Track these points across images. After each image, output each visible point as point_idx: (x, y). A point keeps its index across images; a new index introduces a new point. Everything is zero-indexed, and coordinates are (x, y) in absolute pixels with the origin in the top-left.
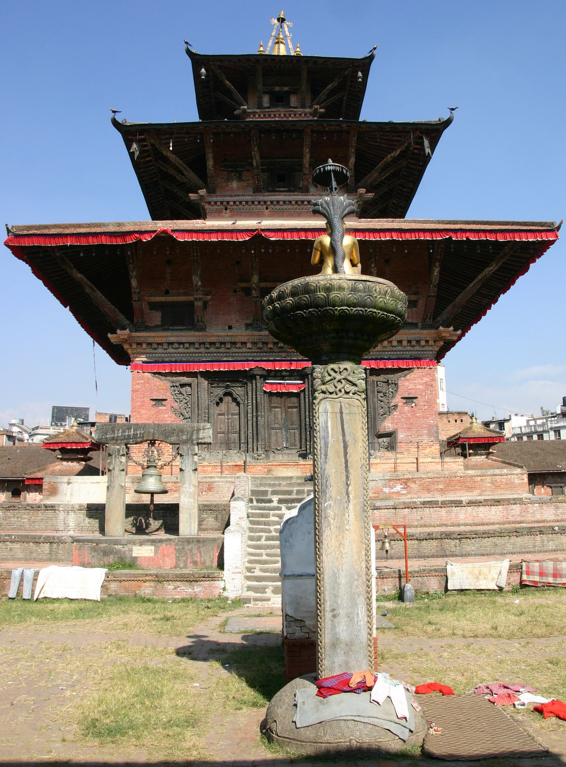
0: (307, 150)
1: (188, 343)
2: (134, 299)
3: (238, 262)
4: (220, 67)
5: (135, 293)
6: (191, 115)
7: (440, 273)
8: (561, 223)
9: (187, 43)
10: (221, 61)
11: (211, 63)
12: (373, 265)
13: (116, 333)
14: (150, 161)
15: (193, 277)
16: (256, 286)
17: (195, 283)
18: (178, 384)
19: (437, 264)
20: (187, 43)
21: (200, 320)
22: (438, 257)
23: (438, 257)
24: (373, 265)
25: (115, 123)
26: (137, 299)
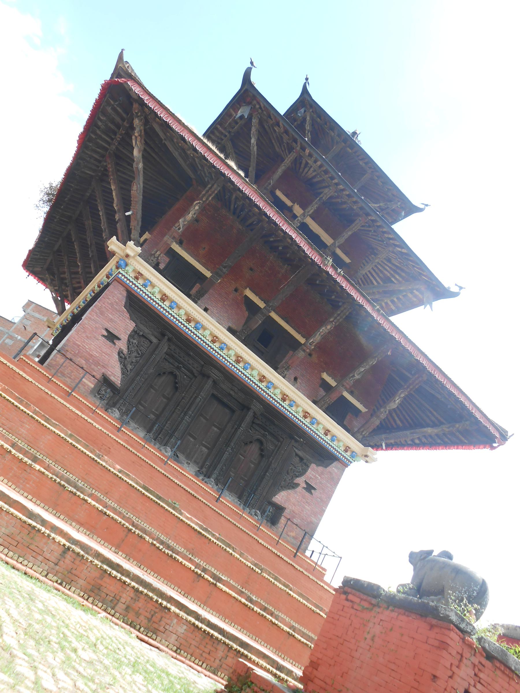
8: (513, 434)
14: (226, 136)
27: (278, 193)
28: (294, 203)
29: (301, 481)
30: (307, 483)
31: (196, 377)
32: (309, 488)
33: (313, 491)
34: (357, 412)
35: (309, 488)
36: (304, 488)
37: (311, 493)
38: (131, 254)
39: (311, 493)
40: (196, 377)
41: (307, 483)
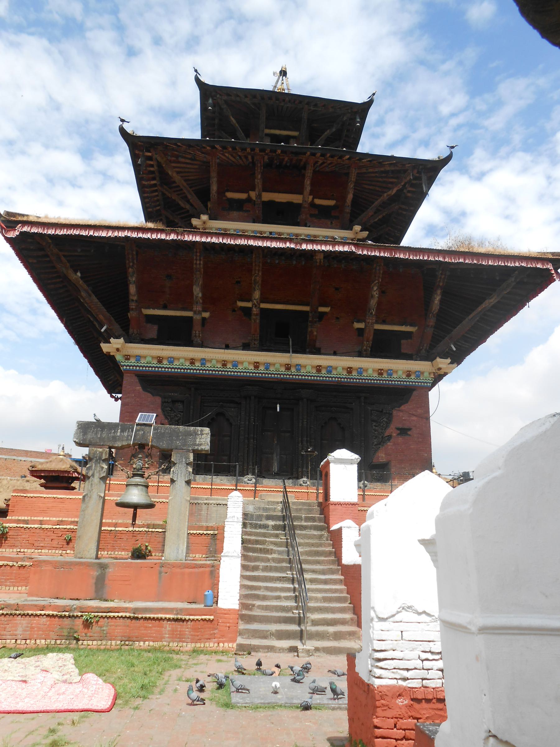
0: (309, 182)
1: (183, 358)
2: (132, 307)
3: (238, 282)
4: (226, 102)
5: (133, 300)
6: (197, 135)
7: (441, 301)
9: (196, 71)
10: (228, 95)
11: (218, 96)
12: (375, 288)
13: (110, 343)
14: (155, 185)
15: (194, 287)
16: (257, 302)
17: (195, 293)
18: (170, 400)
19: (439, 292)
20: (196, 71)
21: (197, 335)
22: (441, 284)
23: (441, 284)
24: (375, 288)
25: (123, 131)
26: (134, 307)
27: (230, 195)
28: (247, 192)
29: (392, 430)
30: (398, 429)
31: (240, 403)
32: (403, 431)
33: (409, 433)
34: (408, 335)
35: (403, 431)
36: (398, 434)
37: (408, 434)
38: (119, 346)
39: (410, 435)
40: (240, 403)
41: (398, 429)
